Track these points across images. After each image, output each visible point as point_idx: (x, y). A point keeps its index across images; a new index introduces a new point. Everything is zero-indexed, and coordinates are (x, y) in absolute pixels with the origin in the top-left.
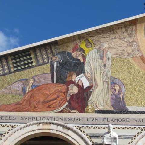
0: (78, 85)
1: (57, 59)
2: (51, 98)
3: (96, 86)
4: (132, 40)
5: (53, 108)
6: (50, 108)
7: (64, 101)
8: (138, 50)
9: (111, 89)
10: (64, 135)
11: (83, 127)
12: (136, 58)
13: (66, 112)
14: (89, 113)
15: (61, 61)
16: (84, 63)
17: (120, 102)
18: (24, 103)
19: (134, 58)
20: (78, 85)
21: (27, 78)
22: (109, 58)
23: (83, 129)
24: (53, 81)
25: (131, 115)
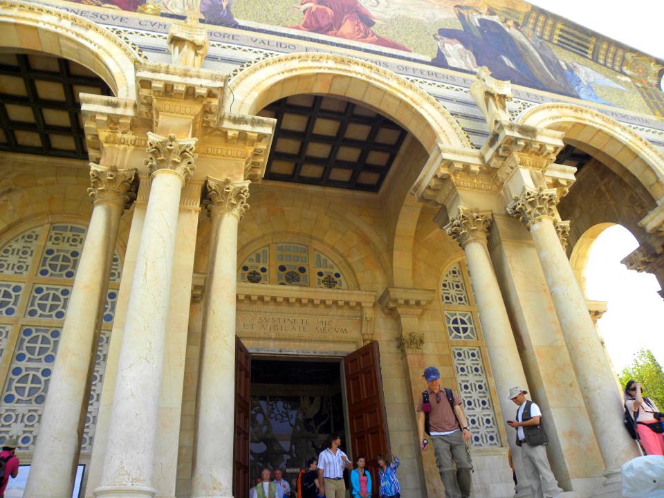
10: (74, 36)
11: (125, 31)
13: (89, 4)
14: (146, 13)
17: (220, 11)
23: (123, 35)
25: (244, 31)
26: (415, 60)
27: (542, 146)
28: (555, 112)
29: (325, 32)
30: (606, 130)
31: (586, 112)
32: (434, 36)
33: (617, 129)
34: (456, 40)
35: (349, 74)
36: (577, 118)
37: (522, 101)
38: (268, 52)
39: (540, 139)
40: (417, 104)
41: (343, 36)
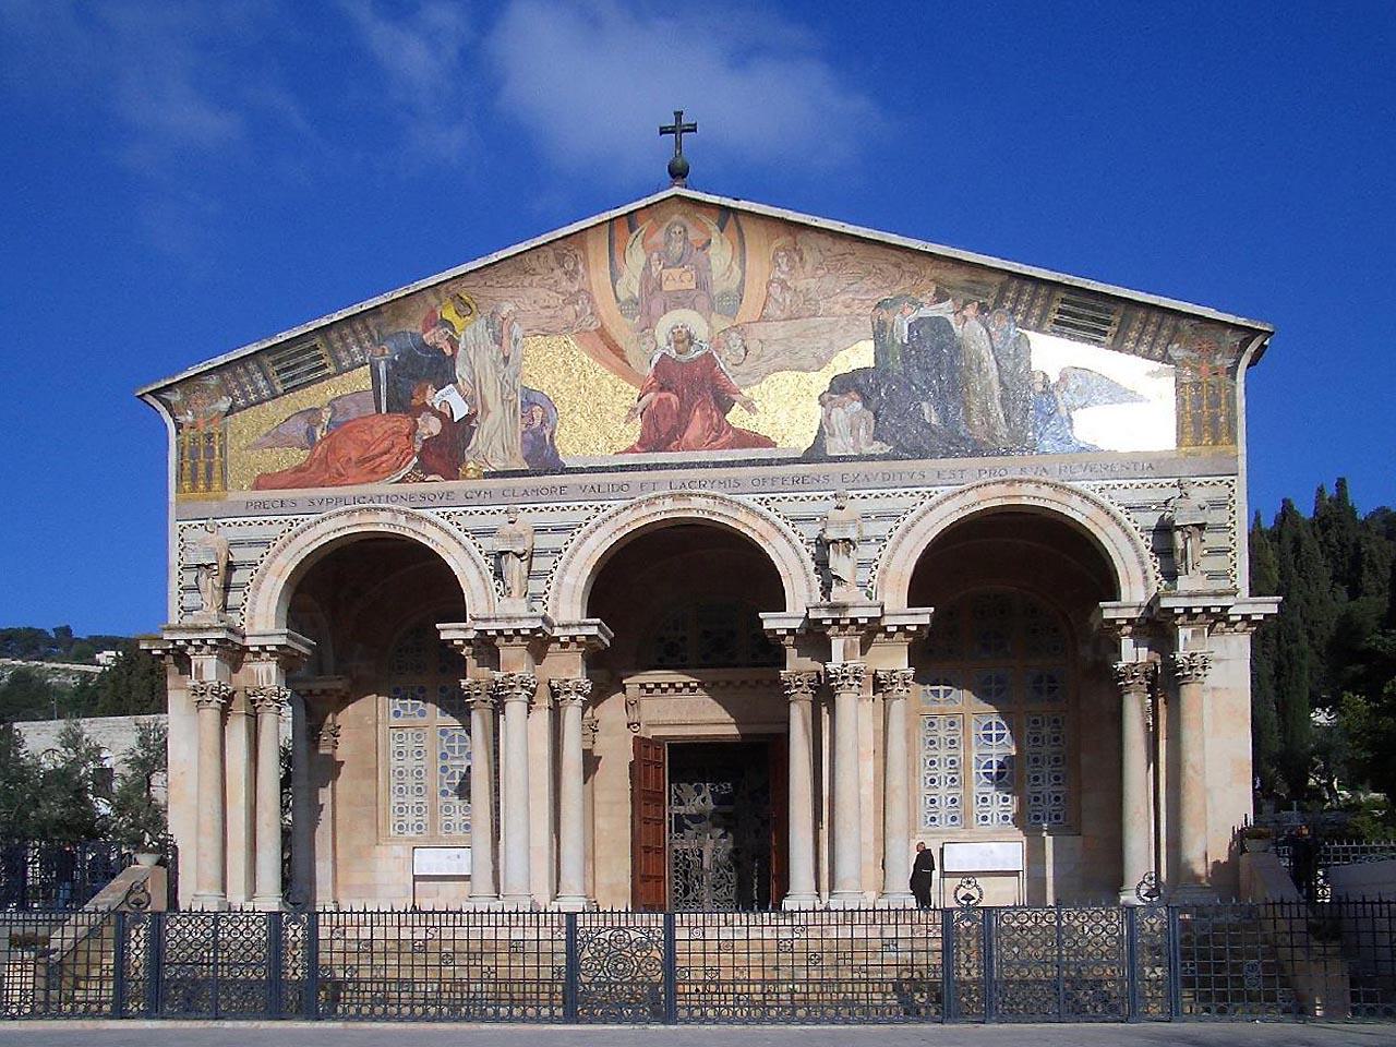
0: (440, 415)
1: (387, 352)
2: (376, 452)
3: (485, 414)
4: (576, 288)
5: (383, 472)
6: (374, 474)
7: (408, 454)
8: (592, 314)
9: (522, 417)
12: (587, 335)
15: (396, 358)
16: (453, 356)
18: (312, 469)
19: (581, 335)
20: (440, 415)
21: (317, 406)
22: (516, 340)
24: (379, 410)
26: (781, 462)
27: (854, 621)
28: (972, 496)
29: (664, 450)
30: (1054, 506)
31: (1030, 481)
32: (819, 398)
33: (1075, 500)
34: (853, 395)
35: (689, 515)
36: (1005, 497)
37: (923, 490)
38: (597, 504)
39: (852, 613)
40: (765, 540)
41: (688, 448)
